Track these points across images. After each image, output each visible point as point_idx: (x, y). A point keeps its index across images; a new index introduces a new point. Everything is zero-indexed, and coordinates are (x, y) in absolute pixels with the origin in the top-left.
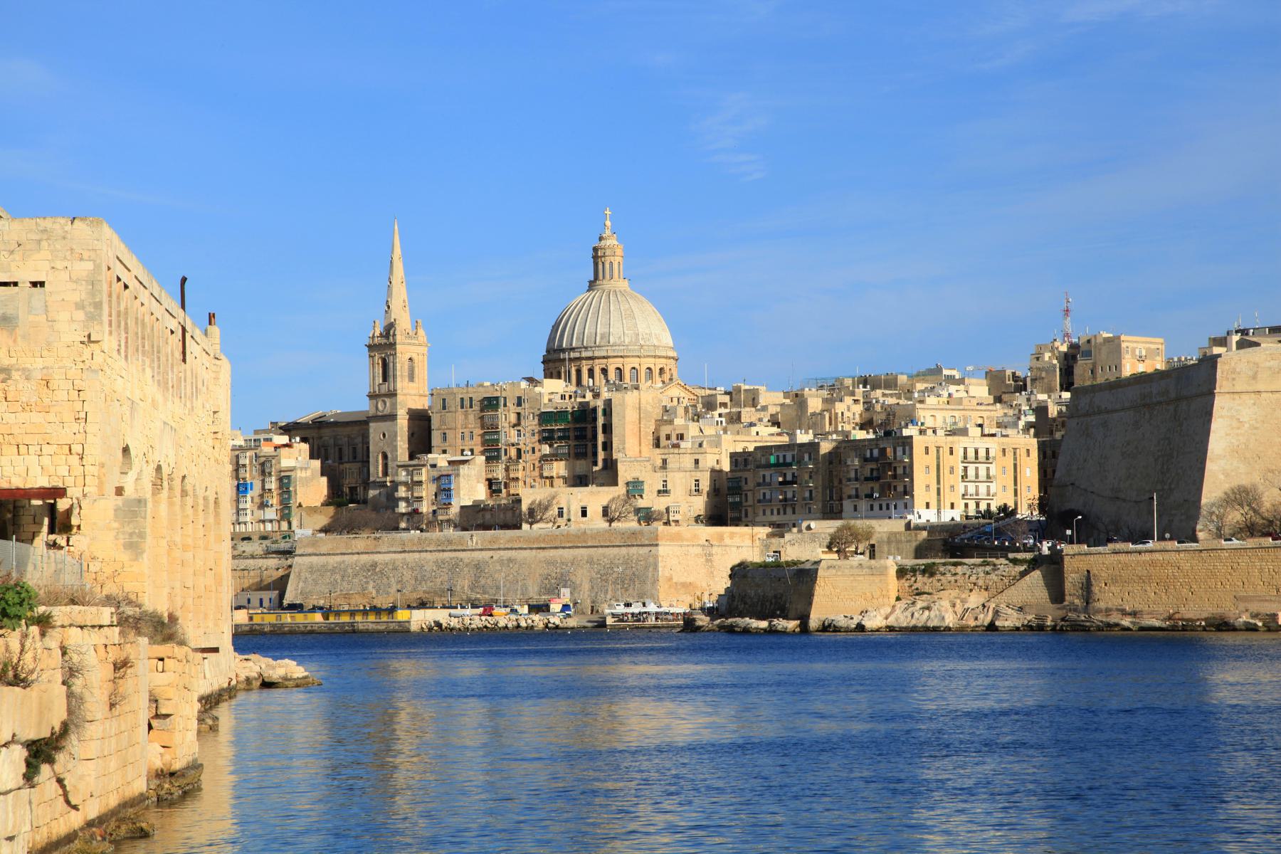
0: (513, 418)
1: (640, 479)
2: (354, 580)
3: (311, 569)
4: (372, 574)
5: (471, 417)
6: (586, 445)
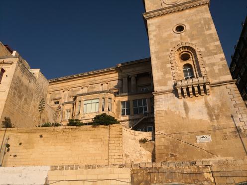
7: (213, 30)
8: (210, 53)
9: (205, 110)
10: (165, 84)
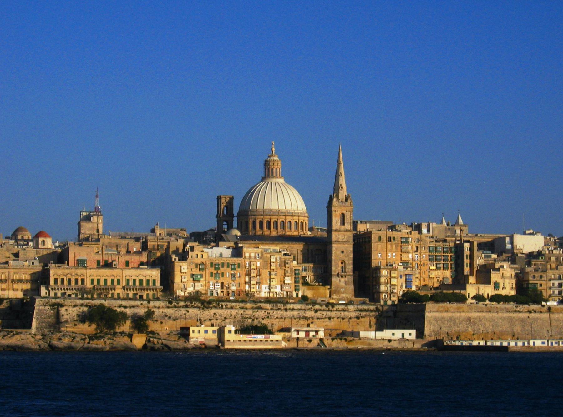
0: (415, 248)
1: (497, 282)
2: (461, 326)
3: (436, 319)
4: (469, 323)
5: (394, 246)
6: (448, 264)
7: (352, 256)
8: (349, 264)
9: (344, 282)
10: (335, 272)
